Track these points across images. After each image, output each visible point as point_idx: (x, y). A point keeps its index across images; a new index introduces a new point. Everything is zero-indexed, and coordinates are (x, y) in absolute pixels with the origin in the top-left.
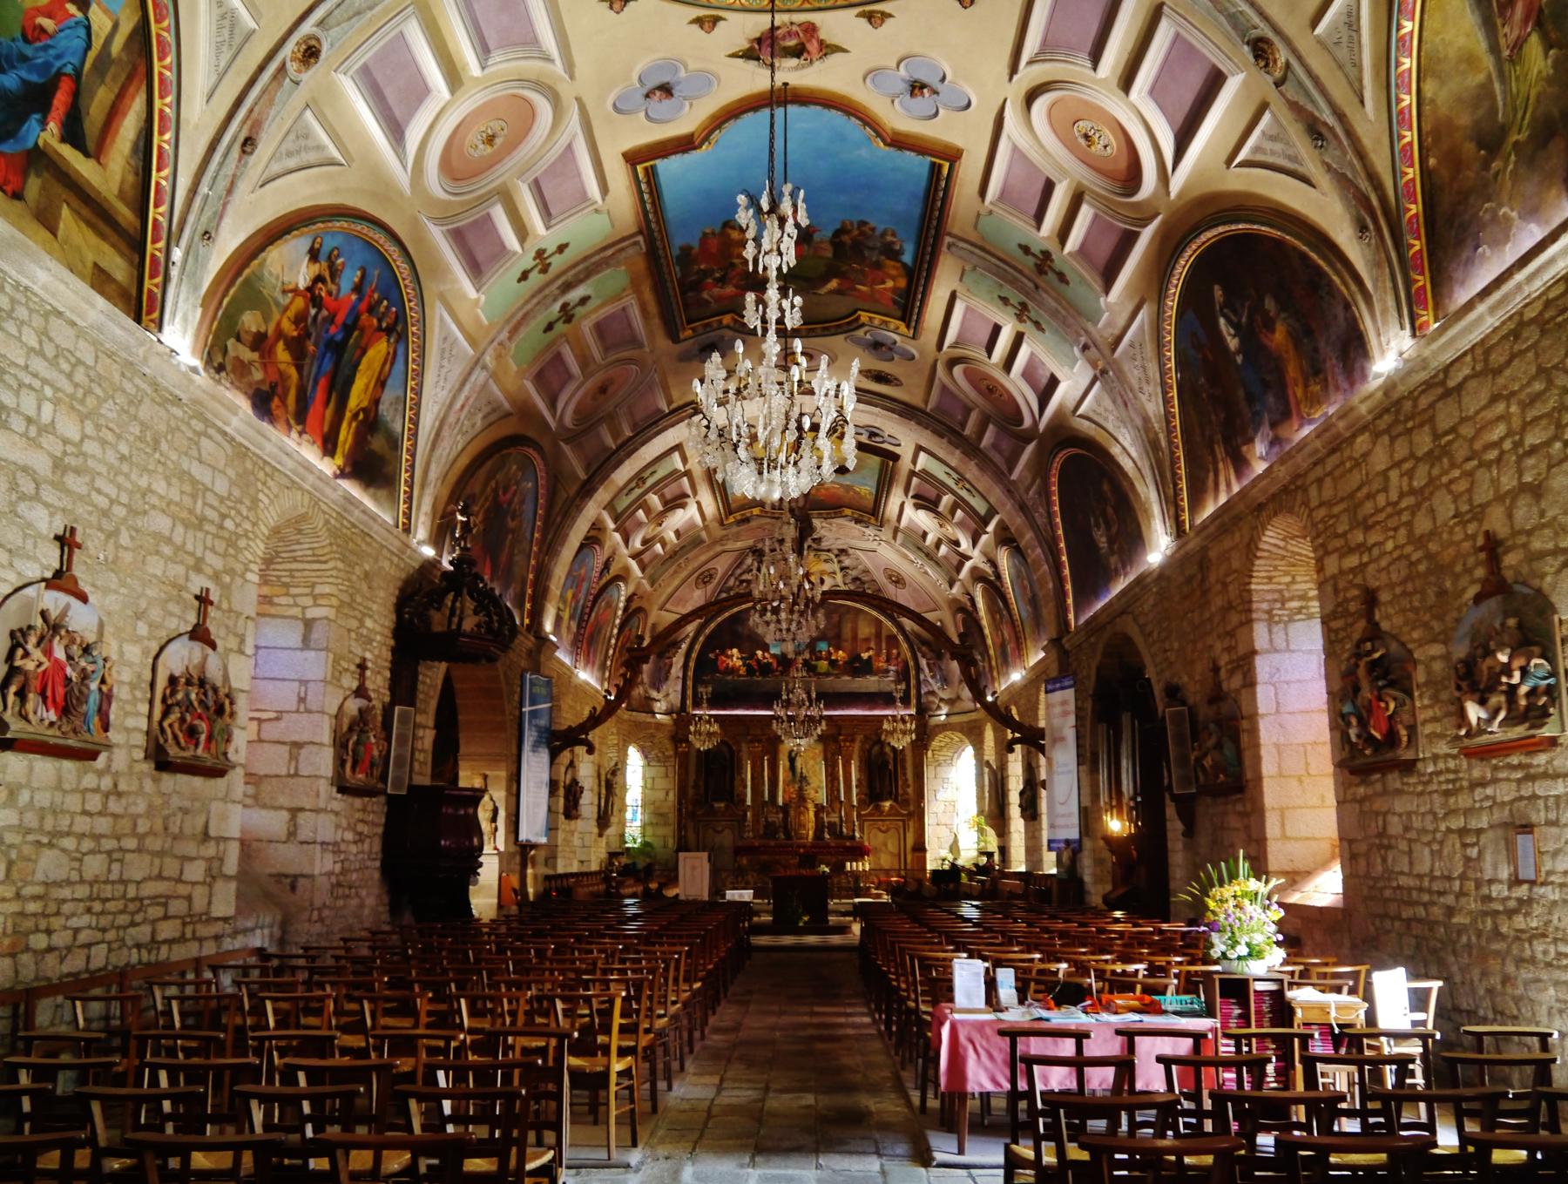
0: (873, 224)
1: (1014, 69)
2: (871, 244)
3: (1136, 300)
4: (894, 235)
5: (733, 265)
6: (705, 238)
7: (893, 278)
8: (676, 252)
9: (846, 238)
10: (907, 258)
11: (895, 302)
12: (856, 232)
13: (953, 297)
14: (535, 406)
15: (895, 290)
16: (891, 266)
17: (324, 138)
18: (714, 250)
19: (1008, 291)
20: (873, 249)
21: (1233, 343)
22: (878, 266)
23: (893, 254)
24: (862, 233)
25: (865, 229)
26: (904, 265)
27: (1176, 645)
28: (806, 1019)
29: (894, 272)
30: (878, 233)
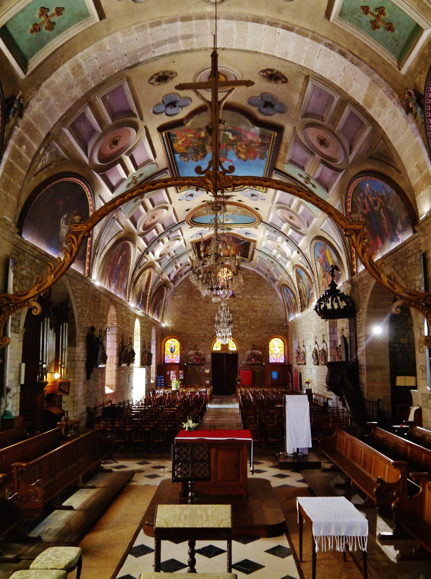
0: (193, 162)
1: (174, 211)
2: (192, 154)
3: (124, 226)
4: (185, 161)
5: (246, 145)
6: (254, 158)
7: (179, 145)
8: (265, 159)
9: (201, 154)
10: (177, 156)
11: (175, 136)
12: (198, 157)
13: (155, 156)
14: (338, 184)
15: (178, 141)
16: (182, 149)
17: (324, 224)
18: (252, 153)
19: (143, 178)
20: (191, 153)
21: (119, 263)
22: (187, 148)
23: (184, 155)
24: (196, 157)
25: (195, 159)
26: (177, 153)
27: (88, 312)
28: (220, 420)
29: (180, 148)
30: (191, 159)
